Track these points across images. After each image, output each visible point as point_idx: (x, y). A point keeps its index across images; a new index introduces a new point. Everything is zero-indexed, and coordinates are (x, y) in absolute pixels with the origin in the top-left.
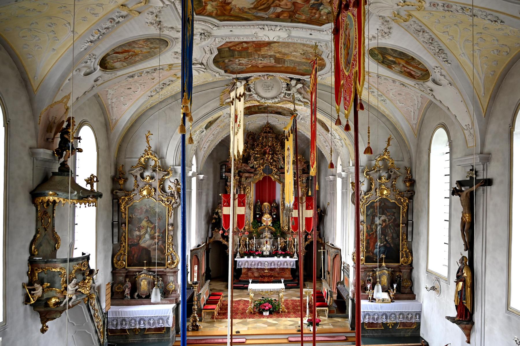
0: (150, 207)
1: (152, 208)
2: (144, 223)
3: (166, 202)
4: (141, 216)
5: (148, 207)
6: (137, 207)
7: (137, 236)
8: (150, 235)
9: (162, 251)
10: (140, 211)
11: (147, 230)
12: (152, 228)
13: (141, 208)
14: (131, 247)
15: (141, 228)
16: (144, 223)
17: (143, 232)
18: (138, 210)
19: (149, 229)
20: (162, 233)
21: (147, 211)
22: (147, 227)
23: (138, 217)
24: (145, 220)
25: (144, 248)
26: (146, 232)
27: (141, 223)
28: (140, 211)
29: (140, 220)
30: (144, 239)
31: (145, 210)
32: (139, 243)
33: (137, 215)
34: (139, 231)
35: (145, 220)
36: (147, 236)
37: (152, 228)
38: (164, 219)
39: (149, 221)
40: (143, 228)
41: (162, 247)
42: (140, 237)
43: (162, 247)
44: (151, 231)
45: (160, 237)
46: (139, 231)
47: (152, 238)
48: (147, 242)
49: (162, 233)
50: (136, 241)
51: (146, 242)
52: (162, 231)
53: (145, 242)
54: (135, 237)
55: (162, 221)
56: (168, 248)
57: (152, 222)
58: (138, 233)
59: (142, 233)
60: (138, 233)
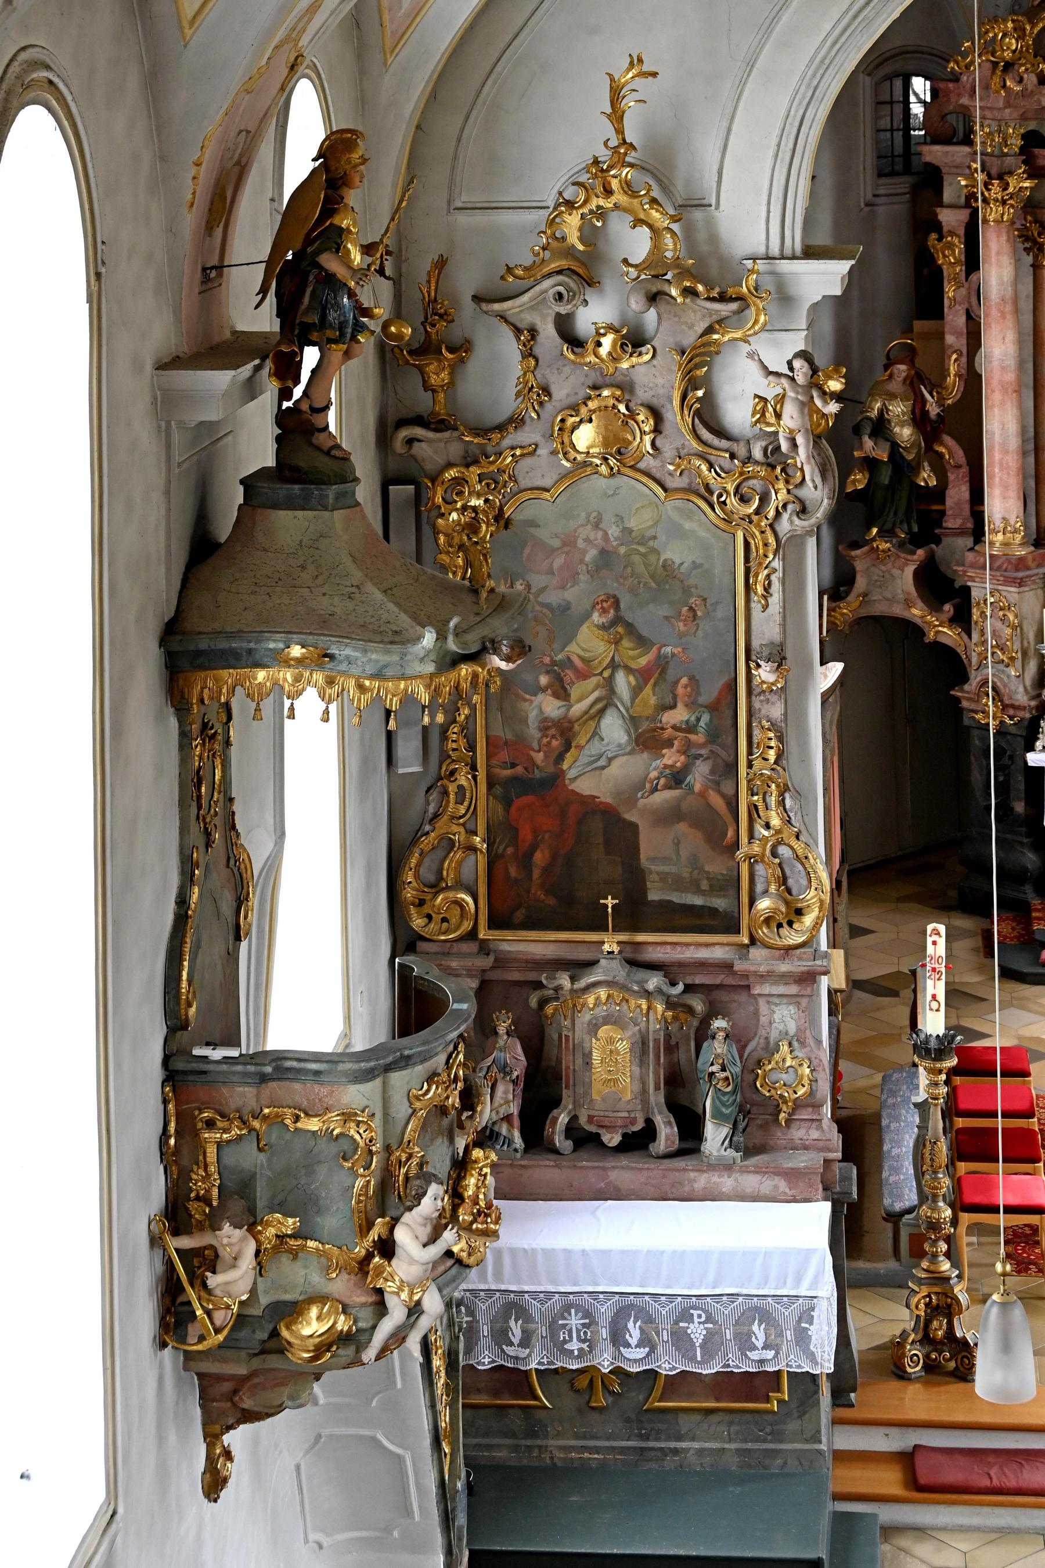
0: (627, 531)
1: (643, 541)
2: (590, 642)
3: (733, 502)
4: (570, 594)
5: (614, 532)
6: (542, 533)
7: (546, 725)
8: (634, 721)
9: (718, 830)
10: (559, 561)
11: (610, 684)
12: (644, 676)
13: (569, 543)
14: (507, 803)
15: (569, 675)
16: (590, 642)
17: (584, 697)
18: (552, 551)
19: (623, 683)
20: (713, 708)
21: (606, 556)
22: (613, 665)
23: (553, 597)
24: (596, 617)
25: (591, 809)
26: (608, 700)
27: (571, 637)
28: (559, 561)
29: (565, 621)
30: (594, 748)
31: (591, 554)
32: (562, 773)
33: (547, 585)
34: (561, 691)
35: (596, 617)
36: (613, 729)
37: (644, 676)
38: (721, 612)
39: (621, 626)
40: (583, 676)
41: (717, 802)
42: (565, 733)
43: (717, 802)
44: (636, 691)
45: (699, 738)
46: (561, 691)
47: (648, 739)
48: (616, 769)
49: (713, 708)
50: (539, 757)
51: (607, 764)
52: (710, 692)
53: (600, 765)
54: (533, 731)
55: (705, 626)
56: (753, 808)
57: (645, 632)
58: (551, 707)
59: (578, 709)
60: (551, 707)
